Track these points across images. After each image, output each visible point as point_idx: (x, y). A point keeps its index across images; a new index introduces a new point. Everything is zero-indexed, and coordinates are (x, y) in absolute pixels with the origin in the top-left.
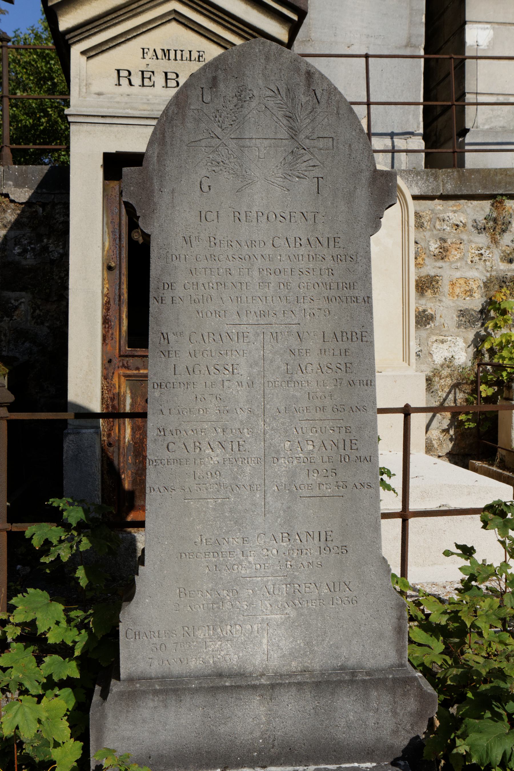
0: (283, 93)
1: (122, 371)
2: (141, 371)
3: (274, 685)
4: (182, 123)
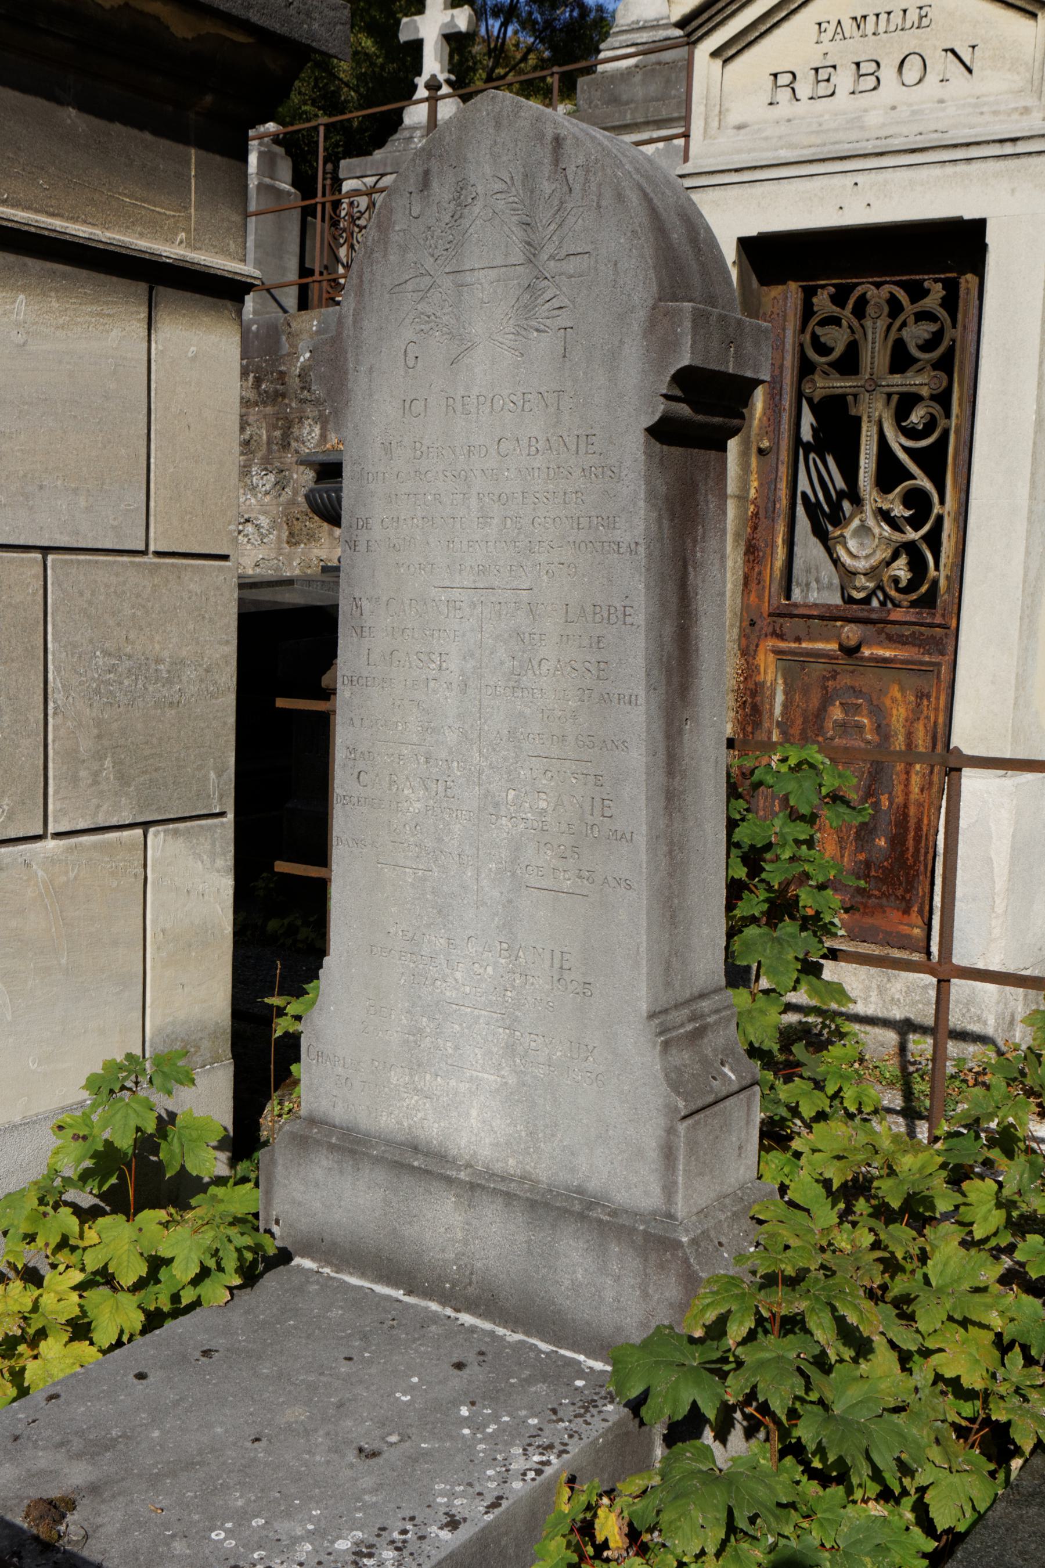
0: (518, 184)
1: (771, 643)
2: (804, 645)
3: (478, 1185)
4: (384, 256)
